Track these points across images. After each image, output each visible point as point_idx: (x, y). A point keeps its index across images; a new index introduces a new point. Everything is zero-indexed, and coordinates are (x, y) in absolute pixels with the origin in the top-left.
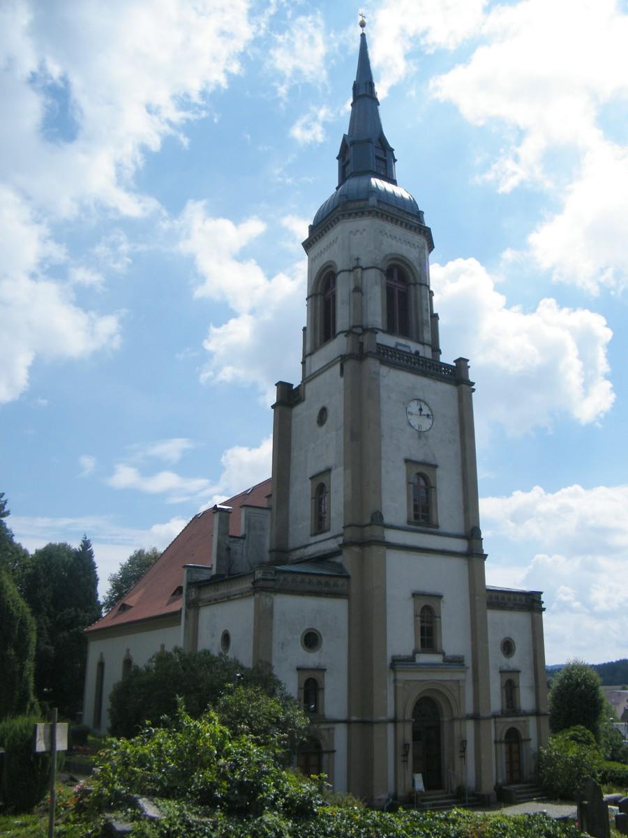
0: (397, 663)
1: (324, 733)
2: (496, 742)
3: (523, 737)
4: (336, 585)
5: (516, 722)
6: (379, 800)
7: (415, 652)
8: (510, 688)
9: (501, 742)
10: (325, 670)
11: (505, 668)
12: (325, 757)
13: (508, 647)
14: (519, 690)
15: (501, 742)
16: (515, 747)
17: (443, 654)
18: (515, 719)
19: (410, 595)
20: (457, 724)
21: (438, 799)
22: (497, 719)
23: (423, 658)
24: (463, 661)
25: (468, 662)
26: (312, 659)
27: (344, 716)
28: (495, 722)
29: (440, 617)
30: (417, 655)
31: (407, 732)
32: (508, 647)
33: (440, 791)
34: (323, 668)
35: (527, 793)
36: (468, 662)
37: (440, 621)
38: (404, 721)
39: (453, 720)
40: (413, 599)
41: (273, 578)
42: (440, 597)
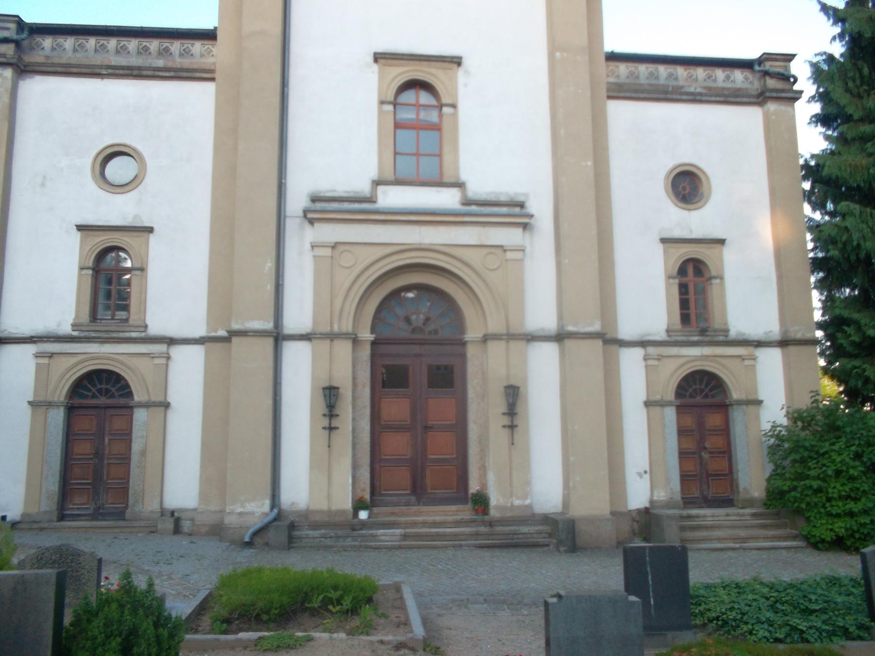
0: (324, 208)
1: (142, 365)
2: (648, 404)
3: (735, 395)
4: (185, 53)
5: (706, 357)
6: (240, 514)
7: (377, 183)
8: (694, 277)
9: (662, 404)
10: (150, 230)
11: (677, 233)
12: (140, 416)
13: (687, 185)
14: (722, 284)
15: (662, 404)
16: (714, 420)
17: (460, 185)
18: (707, 351)
19: (370, 59)
20: (495, 349)
21: (435, 524)
22: (651, 350)
23: (393, 197)
24: (521, 205)
25: (541, 207)
26: (116, 210)
27: (200, 331)
28: (646, 359)
29: (454, 106)
30: (381, 189)
31: (349, 367)
32: (687, 185)
33: (453, 508)
34: (147, 224)
35: (766, 538)
36: (541, 207)
37: (455, 116)
38: (332, 337)
39: (486, 339)
40: (375, 67)
41: (15, 37)
42: (460, 58)
